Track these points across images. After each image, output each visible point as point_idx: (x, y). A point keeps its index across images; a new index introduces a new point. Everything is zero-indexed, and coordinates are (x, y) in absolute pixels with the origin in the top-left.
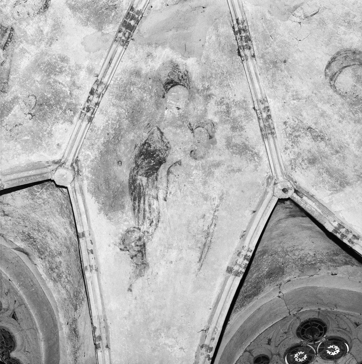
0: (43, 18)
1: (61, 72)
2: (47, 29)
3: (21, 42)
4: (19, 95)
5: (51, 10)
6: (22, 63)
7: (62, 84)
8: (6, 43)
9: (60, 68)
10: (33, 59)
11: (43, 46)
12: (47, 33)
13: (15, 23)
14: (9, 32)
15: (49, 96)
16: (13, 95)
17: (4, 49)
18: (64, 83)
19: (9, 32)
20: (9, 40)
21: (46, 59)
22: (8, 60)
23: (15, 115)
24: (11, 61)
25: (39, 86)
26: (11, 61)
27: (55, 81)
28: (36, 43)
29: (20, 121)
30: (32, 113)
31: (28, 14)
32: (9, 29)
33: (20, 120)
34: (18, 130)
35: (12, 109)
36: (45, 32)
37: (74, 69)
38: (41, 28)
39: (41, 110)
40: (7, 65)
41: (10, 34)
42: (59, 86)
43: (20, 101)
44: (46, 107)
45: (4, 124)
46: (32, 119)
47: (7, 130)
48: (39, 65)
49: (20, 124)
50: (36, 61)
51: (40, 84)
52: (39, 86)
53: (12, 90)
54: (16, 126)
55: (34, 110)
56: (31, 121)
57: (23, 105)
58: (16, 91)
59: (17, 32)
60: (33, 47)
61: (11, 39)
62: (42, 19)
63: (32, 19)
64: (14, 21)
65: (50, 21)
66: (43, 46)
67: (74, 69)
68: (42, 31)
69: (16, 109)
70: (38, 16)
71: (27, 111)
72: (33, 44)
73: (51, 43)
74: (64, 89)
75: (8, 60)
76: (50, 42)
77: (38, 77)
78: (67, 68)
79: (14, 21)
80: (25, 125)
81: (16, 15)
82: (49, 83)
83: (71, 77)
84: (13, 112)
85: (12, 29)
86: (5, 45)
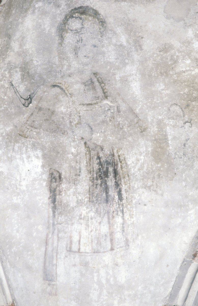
0: (109, 34)
1: (176, 62)
2: (123, 39)
3: (114, 74)
4: (160, 117)
5: (110, 20)
6: (134, 89)
7: (187, 71)
8: (103, 90)
9: (171, 59)
10: (139, 76)
11: (136, 56)
12: (128, 42)
13: (93, 67)
14: (95, 80)
15: (186, 90)
16: (154, 124)
17: (106, 97)
18: (188, 68)
19: (95, 80)
20: (103, 85)
21: (150, 64)
22: (120, 101)
23: (174, 138)
24: (123, 99)
25: (168, 92)
26: (123, 99)
27: (179, 74)
28: (127, 61)
29: (183, 138)
30: (187, 120)
31: (95, 46)
32: (93, 77)
33: (183, 136)
34: (190, 147)
35: (166, 135)
36: (125, 44)
37: (184, 48)
38: (119, 44)
39: (192, 110)
40: (123, 107)
41: (98, 80)
42: (185, 76)
43: (166, 121)
44: (194, 103)
45: (173, 157)
46: (193, 125)
47: (181, 158)
48: (150, 76)
49: (187, 140)
50: (143, 75)
51: (167, 90)
52: (168, 92)
53: (150, 120)
54: (184, 145)
55: (186, 116)
56: (193, 128)
57: (171, 122)
58: (154, 117)
59: (103, 71)
60: (128, 68)
61: (103, 83)
62: (110, 36)
63: (103, 46)
64: (90, 66)
65: (119, 30)
66: (136, 56)
67: (184, 48)
68: (121, 45)
69: (170, 131)
70: (104, 37)
71: (182, 122)
72: (125, 64)
73: (140, 46)
74: (193, 73)
75: (120, 101)
76: (138, 44)
77: (160, 86)
78: (177, 54)
79: (90, 66)
80: (191, 135)
81: (85, 60)
82: (175, 81)
83: (189, 57)
84: (170, 138)
85: (95, 74)
86: (104, 93)
